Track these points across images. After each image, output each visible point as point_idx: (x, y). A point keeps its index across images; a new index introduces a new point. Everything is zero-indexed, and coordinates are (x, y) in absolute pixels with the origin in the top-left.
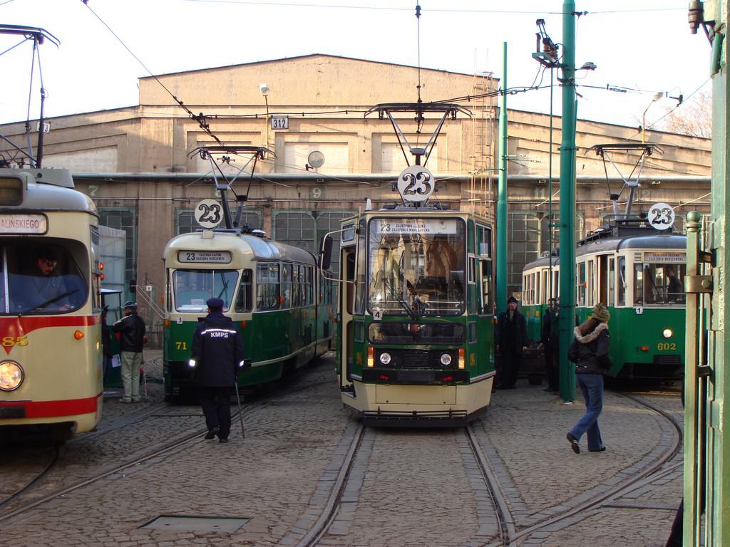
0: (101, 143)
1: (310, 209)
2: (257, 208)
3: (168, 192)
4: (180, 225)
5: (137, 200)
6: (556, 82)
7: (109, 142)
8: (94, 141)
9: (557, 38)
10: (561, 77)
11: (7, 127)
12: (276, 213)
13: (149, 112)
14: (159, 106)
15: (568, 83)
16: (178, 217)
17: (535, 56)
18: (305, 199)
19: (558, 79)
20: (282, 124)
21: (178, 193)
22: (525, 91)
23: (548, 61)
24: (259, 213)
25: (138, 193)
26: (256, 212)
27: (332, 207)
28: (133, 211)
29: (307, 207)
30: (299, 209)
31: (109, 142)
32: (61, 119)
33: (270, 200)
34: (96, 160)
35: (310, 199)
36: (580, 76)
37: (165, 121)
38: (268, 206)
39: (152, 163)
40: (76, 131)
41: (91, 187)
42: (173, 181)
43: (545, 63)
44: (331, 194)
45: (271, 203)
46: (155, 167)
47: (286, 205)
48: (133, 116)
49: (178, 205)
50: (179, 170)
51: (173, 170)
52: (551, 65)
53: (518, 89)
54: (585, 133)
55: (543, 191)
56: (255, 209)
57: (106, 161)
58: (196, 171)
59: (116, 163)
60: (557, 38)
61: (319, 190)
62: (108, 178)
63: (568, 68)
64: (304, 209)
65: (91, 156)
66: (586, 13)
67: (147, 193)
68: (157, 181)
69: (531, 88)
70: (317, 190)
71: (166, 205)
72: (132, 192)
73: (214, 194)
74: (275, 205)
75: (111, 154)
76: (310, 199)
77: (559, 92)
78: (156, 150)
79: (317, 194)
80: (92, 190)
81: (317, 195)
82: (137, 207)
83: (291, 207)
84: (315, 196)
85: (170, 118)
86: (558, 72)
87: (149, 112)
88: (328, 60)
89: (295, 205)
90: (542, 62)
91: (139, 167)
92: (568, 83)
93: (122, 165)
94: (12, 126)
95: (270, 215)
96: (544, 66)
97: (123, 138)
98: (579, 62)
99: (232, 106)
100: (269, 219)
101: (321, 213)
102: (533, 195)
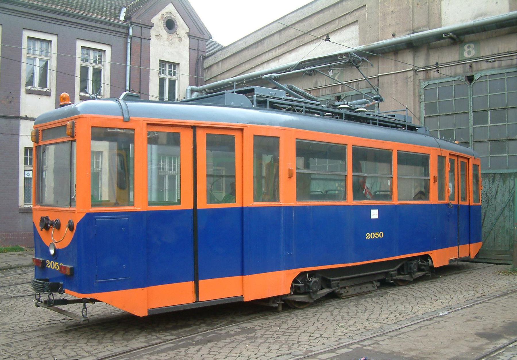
0: (344, 22)
4: (424, 101)
7: (350, 19)
8: (337, 21)
11: (268, 28)
16: (422, 91)
31: (350, 19)
32: (308, 7)
39: (391, 31)
40: (321, 15)
49: (421, 76)
71: (407, 78)
73: (462, 54)
75: (353, 32)
78: (394, 16)
93: (362, 41)
94: (270, 26)
97: (363, 11)
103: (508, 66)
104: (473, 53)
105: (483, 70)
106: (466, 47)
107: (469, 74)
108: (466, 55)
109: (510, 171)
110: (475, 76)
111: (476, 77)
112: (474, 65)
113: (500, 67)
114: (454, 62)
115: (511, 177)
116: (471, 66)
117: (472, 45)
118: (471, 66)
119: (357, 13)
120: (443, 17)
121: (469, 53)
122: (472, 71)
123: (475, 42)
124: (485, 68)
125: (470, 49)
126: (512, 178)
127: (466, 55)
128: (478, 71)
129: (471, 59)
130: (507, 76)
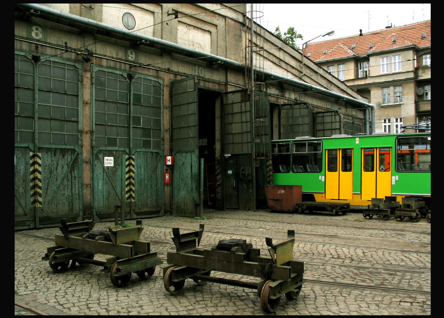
1: (125, 70)
2: (76, 61)
12: (96, 69)
18: (122, 60)
24: (79, 66)
26: (76, 65)
27: (143, 72)
29: (123, 68)
30: (115, 68)
33: (91, 54)
35: (127, 61)
38: (87, 60)
45: (91, 58)
47: (104, 63)
56: (76, 61)
61: (134, 53)
64: (120, 69)
70: (132, 54)
73: (31, 33)
74: (94, 61)
76: (127, 61)
81: (132, 58)
83: (108, 66)
84: (130, 58)
89: (112, 64)
95: (90, 71)
100: (88, 75)
103: (68, 59)
104: (40, 36)
105: (47, 55)
106: (34, 28)
107: (35, 54)
109: (68, 147)
110: (42, 58)
111: (43, 59)
113: (62, 58)
114: (22, 37)
115: (68, 152)
116: (37, 48)
117: (40, 29)
118: (37, 48)
121: (37, 34)
122: (37, 52)
123: (44, 28)
124: (49, 54)
125: (38, 32)
126: (70, 153)
127: (34, 35)
128: (43, 54)
129: (38, 41)
130: (67, 67)
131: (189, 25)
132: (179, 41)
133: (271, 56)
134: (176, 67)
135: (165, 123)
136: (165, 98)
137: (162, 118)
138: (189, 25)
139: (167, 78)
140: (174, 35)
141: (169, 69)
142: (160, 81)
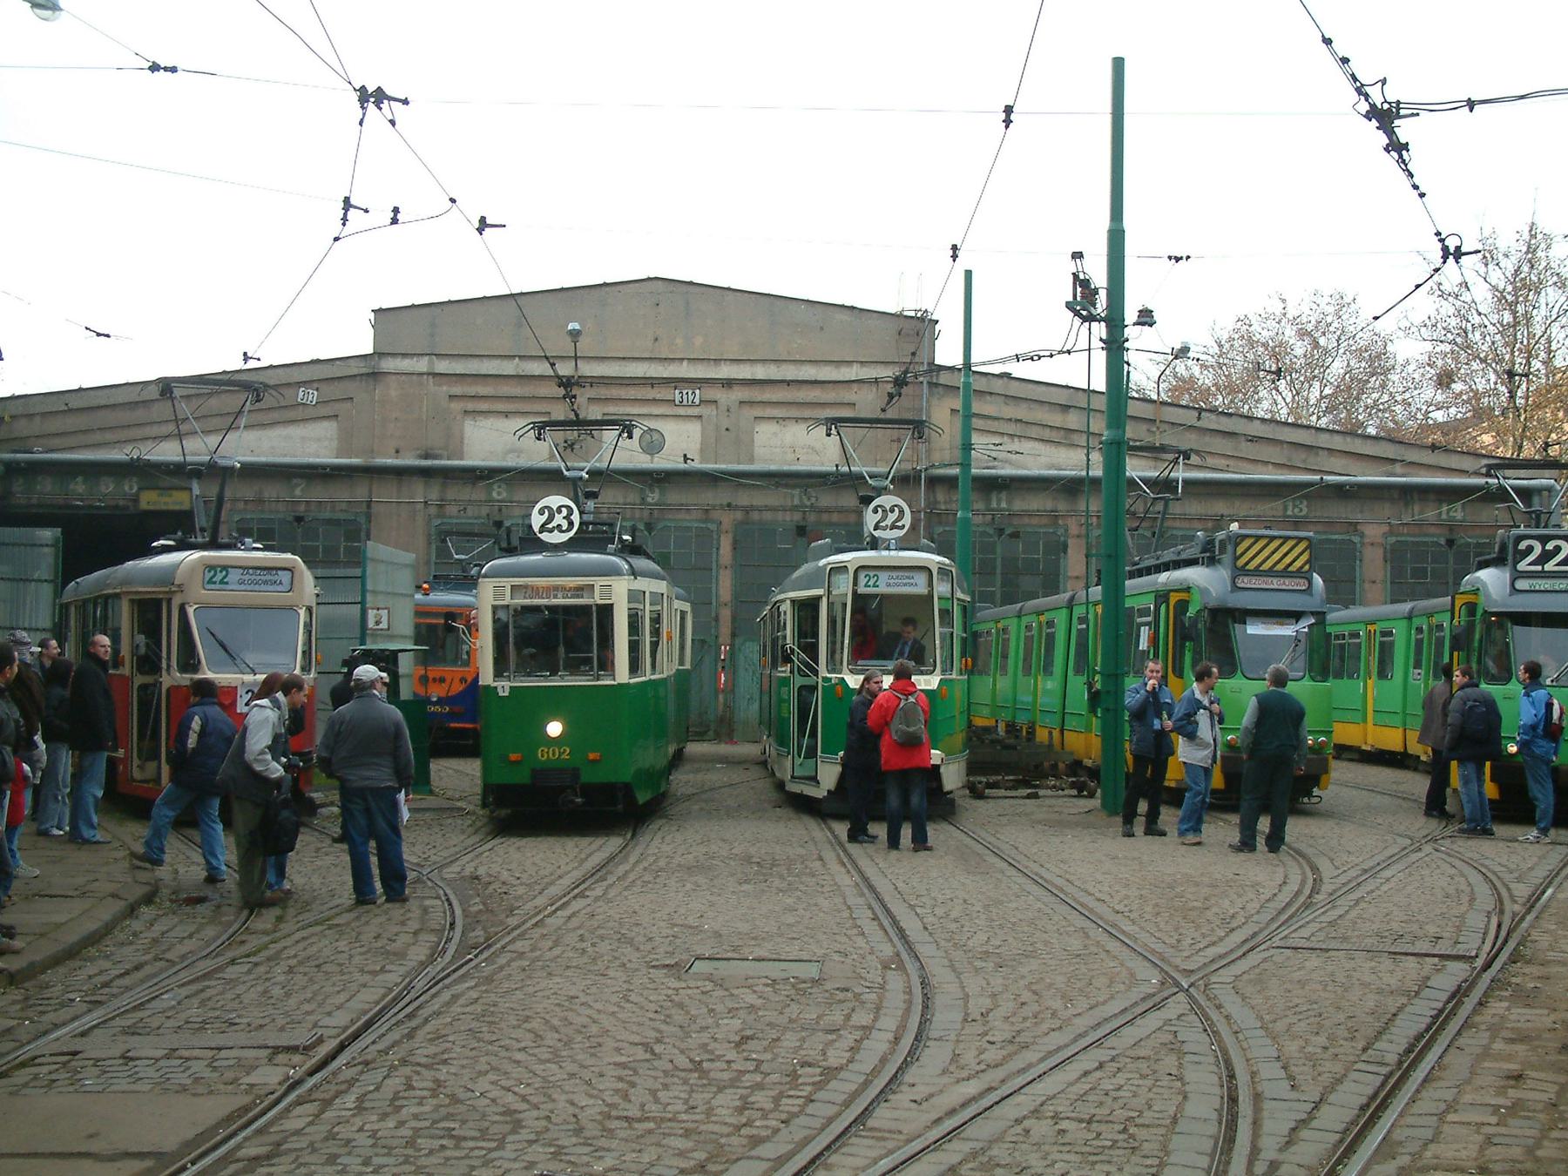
1: (641, 519)
3: (419, 492)
5: (369, 503)
6: (1097, 344)
9: (1100, 279)
10: (1104, 337)
13: (389, 365)
14: (405, 355)
15: (1115, 346)
17: (1069, 306)
19: (1101, 340)
20: (691, 398)
21: (434, 494)
22: (1051, 356)
23: (1084, 313)
25: (370, 491)
28: (362, 520)
29: (637, 516)
34: (303, 438)
36: (1135, 336)
37: (415, 377)
41: (295, 481)
42: (426, 473)
43: (1080, 316)
44: (675, 497)
46: (397, 452)
48: (364, 371)
49: (433, 510)
50: (436, 457)
51: (427, 456)
52: (1090, 319)
53: (1042, 354)
54: (1070, 407)
55: (1004, 495)
57: (319, 440)
58: (462, 459)
59: (335, 444)
60: (1100, 279)
61: (657, 490)
62: (324, 467)
63: (1115, 322)
65: (295, 431)
66: (1188, 257)
67: (385, 494)
68: (400, 473)
69: (1060, 352)
72: (360, 492)
73: (490, 494)
77: (1100, 358)
79: (653, 497)
80: (297, 485)
82: (369, 516)
84: (649, 500)
85: (421, 374)
86: (1100, 330)
87: (389, 365)
88: (671, 287)
90: (1077, 314)
91: (372, 451)
92: (1115, 346)
93: (344, 449)
96: (1077, 321)
97: (348, 405)
98: (1130, 315)
99: (520, 357)
101: (660, 526)
102: (988, 501)
107: (497, 519)
108: (495, 494)
112: (504, 510)
116: (500, 510)
117: (504, 486)
118: (500, 510)
119: (337, 406)
120: (466, 441)
121: (499, 494)
131: (784, 419)
132: (759, 451)
133: (1035, 428)
134: (744, 498)
135: (722, 592)
136: (721, 552)
137: (714, 586)
138: (784, 419)
139: (727, 519)
140: (745, 445)
141: (729, 505)
142: (709, 525)
